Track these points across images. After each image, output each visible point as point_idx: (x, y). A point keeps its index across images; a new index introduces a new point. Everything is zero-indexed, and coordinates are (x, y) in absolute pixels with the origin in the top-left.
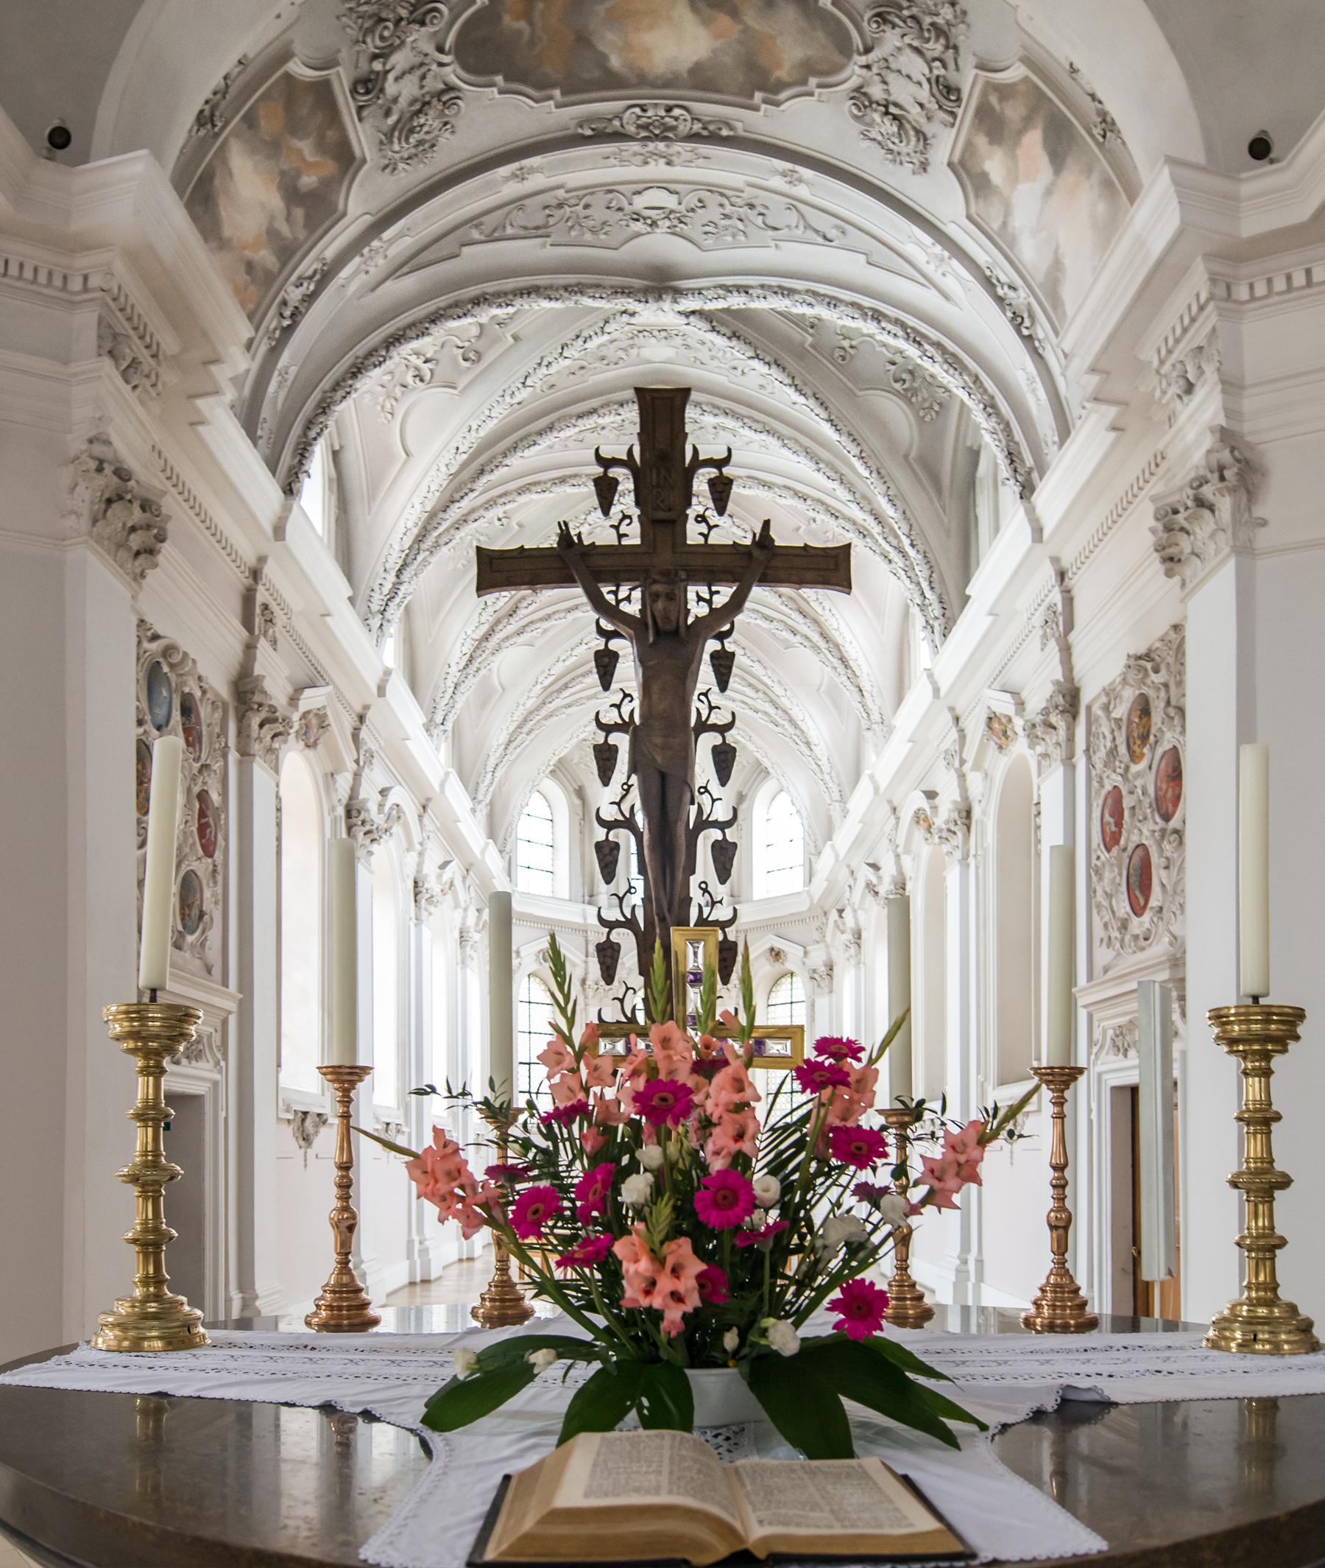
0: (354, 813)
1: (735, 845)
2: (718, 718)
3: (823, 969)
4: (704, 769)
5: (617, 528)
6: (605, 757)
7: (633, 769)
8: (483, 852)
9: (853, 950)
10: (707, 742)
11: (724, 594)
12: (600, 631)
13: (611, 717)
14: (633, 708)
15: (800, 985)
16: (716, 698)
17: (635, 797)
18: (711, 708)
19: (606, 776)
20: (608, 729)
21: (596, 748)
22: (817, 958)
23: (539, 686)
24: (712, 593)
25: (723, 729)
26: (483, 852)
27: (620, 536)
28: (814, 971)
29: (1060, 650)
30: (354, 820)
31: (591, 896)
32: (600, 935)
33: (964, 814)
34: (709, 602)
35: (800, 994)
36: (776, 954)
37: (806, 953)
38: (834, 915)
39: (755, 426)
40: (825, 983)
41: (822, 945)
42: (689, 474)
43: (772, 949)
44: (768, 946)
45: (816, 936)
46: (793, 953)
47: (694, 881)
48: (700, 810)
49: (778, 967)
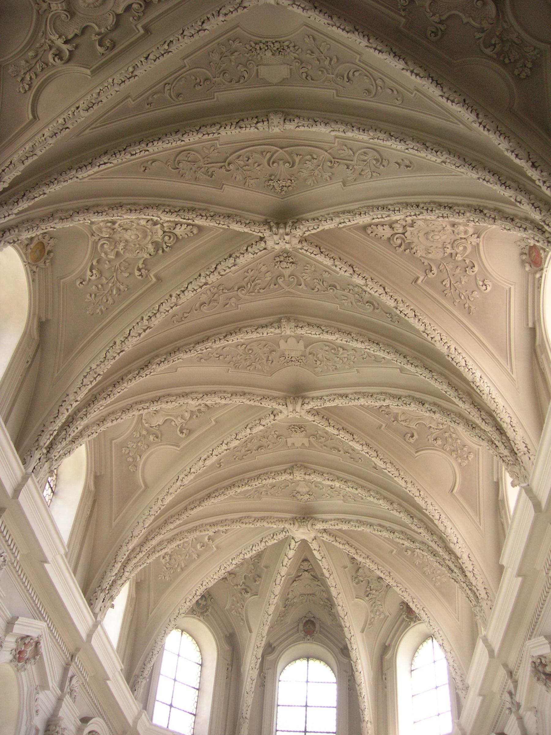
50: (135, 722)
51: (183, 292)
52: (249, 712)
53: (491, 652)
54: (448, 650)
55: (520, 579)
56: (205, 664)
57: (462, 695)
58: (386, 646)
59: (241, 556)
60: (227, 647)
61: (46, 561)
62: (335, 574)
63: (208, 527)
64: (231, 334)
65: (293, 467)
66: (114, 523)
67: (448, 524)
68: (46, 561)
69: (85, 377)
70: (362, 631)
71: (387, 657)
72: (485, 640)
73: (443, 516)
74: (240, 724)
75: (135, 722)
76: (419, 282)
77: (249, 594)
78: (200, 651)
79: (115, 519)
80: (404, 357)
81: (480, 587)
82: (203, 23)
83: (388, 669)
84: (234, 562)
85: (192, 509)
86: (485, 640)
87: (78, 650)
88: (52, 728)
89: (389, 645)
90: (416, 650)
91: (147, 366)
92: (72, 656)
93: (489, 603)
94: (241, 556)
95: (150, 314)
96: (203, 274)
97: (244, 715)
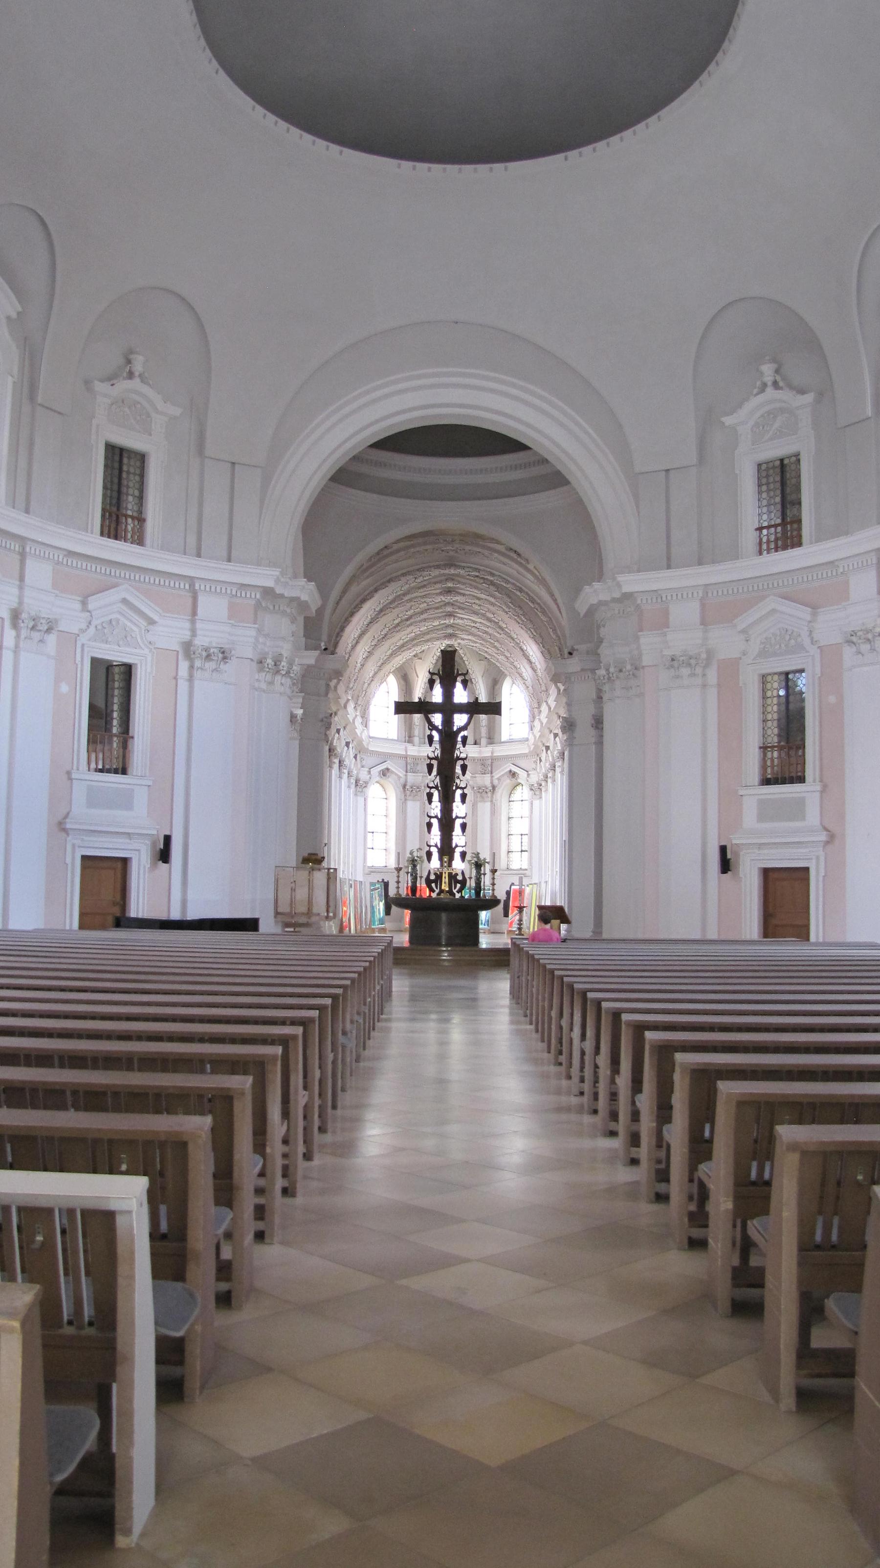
0: (332, 751)
1: (466, 794)
2: (463, 756)
3: (536, 785)
4: (458, 770)
6: (430, 768)
7: (438, 774)
10: (460, 763)
12: (429, 729)
13: (432, 755)
14: (438, 752)
16: (462, 749)
17: (438, 780)
18: (461, 753)
19: (430, 772)
20: (431, 759)
21: (427, 764)
23: (391, 651)
25: (463, 759)
28: (533, 785)
30: (331, 753)
31: (410, 737)
32: (427, 820)
33: (562, 754)
36: (513, 774)
37: (528, 775)
39: (486, 593)
40: (537, 793)
43: (510, 771)
44: (508, 769)
45: (534, 766)
46: (522, 774)
47: (454, 804)
48: (457, 784)
60: (403, 682)
61: (356, 728)
62: (468, 654)
65: (446, 626)
68: (356, 728)
70: (482, 677)
71: (497, 687)
72: (539, 719)
83: (497, 695)
86: (539, 719)
88: (351, 773)
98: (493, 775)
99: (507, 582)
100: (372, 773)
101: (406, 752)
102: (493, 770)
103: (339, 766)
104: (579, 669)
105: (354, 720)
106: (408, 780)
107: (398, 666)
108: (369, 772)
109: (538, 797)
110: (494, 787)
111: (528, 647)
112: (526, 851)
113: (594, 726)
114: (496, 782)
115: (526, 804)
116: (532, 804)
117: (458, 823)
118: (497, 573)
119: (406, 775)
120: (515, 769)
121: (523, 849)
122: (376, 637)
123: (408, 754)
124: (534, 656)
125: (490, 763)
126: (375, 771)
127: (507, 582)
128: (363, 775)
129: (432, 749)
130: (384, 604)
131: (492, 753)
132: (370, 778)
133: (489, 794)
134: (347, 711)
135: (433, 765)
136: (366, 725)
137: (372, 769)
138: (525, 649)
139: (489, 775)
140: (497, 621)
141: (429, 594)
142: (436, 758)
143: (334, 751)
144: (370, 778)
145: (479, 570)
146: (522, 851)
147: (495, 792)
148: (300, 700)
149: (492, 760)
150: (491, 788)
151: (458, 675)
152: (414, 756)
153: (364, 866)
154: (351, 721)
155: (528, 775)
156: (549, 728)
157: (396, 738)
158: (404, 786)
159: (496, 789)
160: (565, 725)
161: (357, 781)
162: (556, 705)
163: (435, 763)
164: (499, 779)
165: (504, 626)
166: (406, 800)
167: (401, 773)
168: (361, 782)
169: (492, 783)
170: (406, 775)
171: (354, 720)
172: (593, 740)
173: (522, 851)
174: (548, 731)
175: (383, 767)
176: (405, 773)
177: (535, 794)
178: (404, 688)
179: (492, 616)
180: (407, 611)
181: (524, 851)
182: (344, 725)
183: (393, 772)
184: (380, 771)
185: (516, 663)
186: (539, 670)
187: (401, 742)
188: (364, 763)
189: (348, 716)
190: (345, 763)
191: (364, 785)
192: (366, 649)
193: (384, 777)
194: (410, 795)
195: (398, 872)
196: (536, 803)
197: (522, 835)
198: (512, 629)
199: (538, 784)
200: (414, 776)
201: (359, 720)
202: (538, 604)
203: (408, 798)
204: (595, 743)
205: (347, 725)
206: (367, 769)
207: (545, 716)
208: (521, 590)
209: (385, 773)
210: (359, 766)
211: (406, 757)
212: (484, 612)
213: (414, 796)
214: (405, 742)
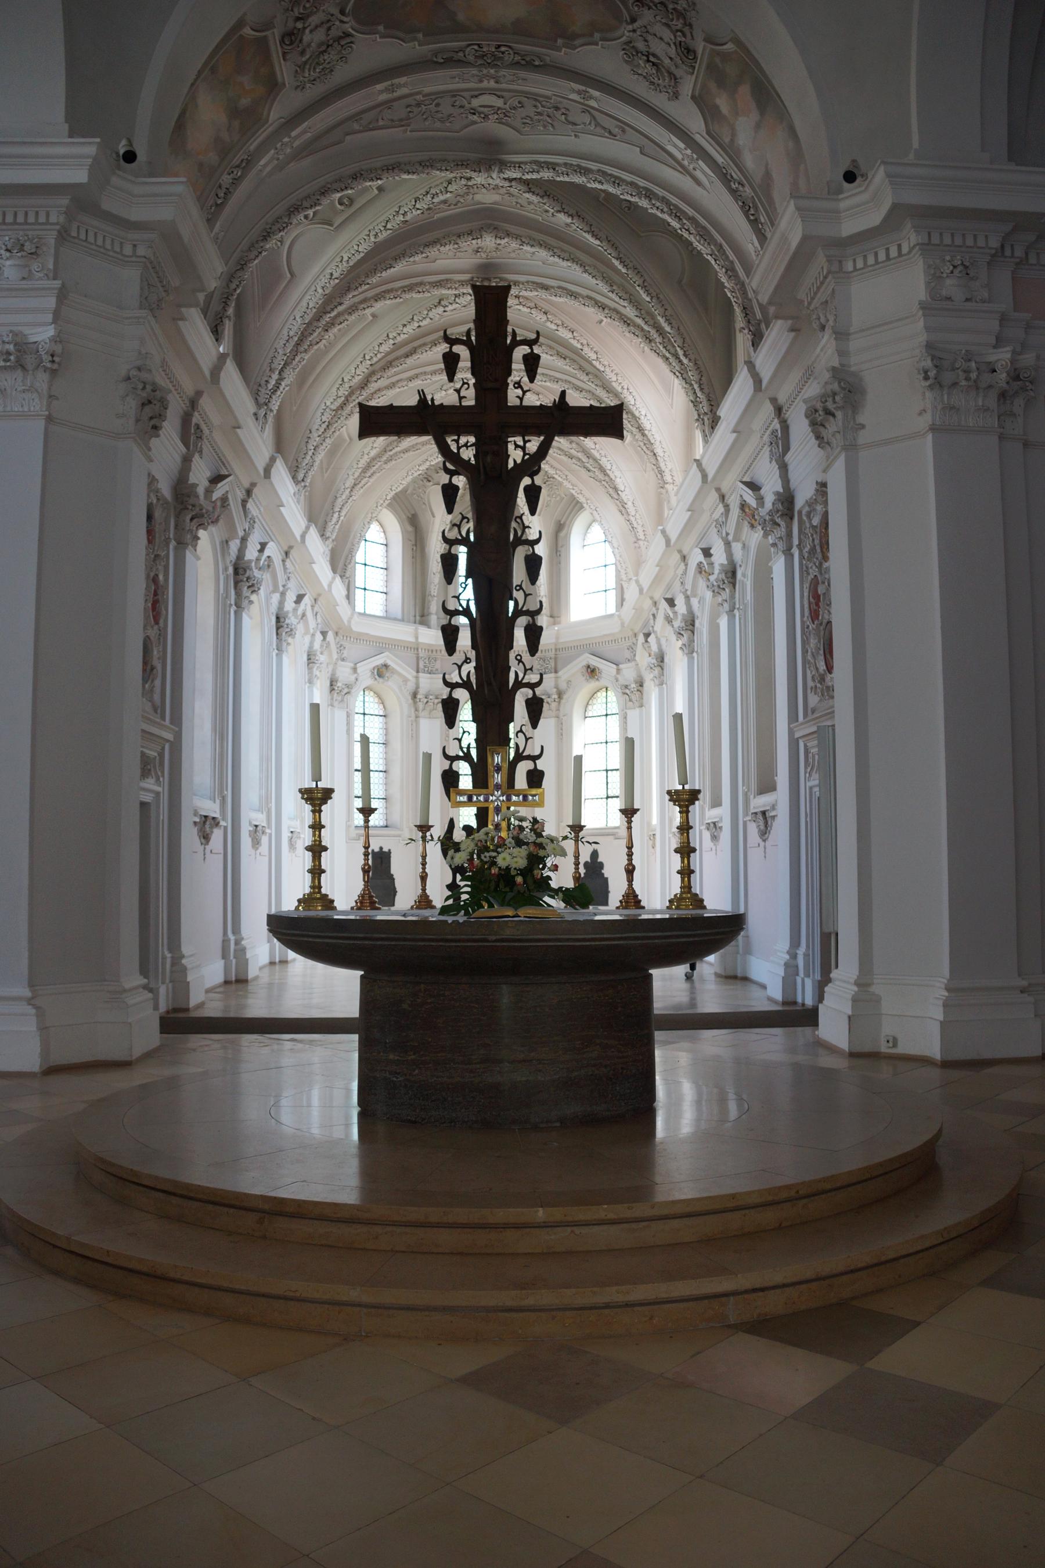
3: (633, 685)
5: (458, 391)
8: (330, 585)
9: (657, 670)
11: (533, 446)
15: (614, 699)
22: (628, 673)
24: (525, 442)
26: (330, 585)
27: (461, 398)
28: (626, 687)
29: (779, 468)
31: (422, 616)
33: (730, 575)
34: (523, 448)
35: (614, 707)
37: (618, 671)
38: (641, 638)
41: (633, 663)
42: (509, 351)
43: (589, 667)
44: (584, 663)
45: (627, 654)
46: (607, 669)
49: (593, 685)
50: (349, 622)
51: (399, 334)
52: (436, 591)
53: (641, 591)
54: (616, 545)
55: (658, 568)
56: (390, 545)
57: (625, 586)
58: (561, 524)
59: (428, 463)
60: (410, 529)
63: (402, 455)
64: (436, 345)
66: (326, 475)
67: (618, 474)
69: (323, 414)
71: (562, 534)
73: (614, 467)
74: (429, 602)
75: (349, 622)
76: (603, 323)
77: (431, 483)
78: (384, 532)
79: (327, 470)
80: (587, 374)
81: (640, 529)
82: (433, 198)
84: (421, 468)
85: (391, 450)
87: (319, 595)
88: (312, 657)
89: (564, 523)
90: (589, 526)
91: (366, 385)
92: (315, 600)
93: (646, 543)
94: (428, 463)
95: (371, 355)
96: (415, 318)
97: (432, 593)
98: (560, 673)
99: (617, 181)
100: (359, 671)
101: (417, 638)
102: (559, 666)
103: (278, 628)
104: (875, 218)
105: (303, 536)
106: (421, 685)
107: (399, 489)
108: (355, 670)
109: (637, 704)
110: (560, 694)
111: (637, 397)
112: (617, 797)
113: (932, 374)
114: (563, 686)
115: (614, 722)
116: (625, 718)
117: (520, 698)
118: (594, 166)
119: (417, 678)
120: (595, 662)
121: (610, 794)
122: (346, 380)
123: (420, 640)
124: (649, 416)
125: (553, 656)
126: (365, 669)
127: (617, 181)
128: (344, 673)
129: (455, 517)
130: (351, 263)
131: (557, 638)
132: (357, 679)
133: (554, 705)
134: (272, 484)
135: (455, 558)
136: (349, 597)
137: (358, 665)
138: (632, 403)
139: (553, 675)
140: (579, 346)
141: (447, 280)
142: (466, 685)
143: (245, 571)
144: (357, 679)
145: (552, 166)
146: (608, 797)
147: (563, 701)
148: (51, 302)
149: (556, 650)
150: (556, 696)
151: (516, 343)
152: (430, 645)
153: (348, 827)
154: (299, 538)
155: (618, 671)
156: (651, 598)
157: (399, 616)
158: (415, 695)
159: (565, 697)
160: (835, 386)
161: (332, 683)
162: (736, 441)
163: (462, 553)
164: (569, 682)
165: (593, 356)
166: (417, 717)
167: (409, 673)
168: (339, 684)
169: (556, 687)
170: (417, 678)
171: (303, 536)
172: (927, 419)
173: (608, 797)
174: (677, 557)
175: (378, 661)
176: (415, 673)
177: (630, 700)
178: (413, 538)
179: (570, 335)
180: (404, 325)
181: (612, 797)
182: (247, 485)
183: (394, 671)
184: (374, 669)
185: (604, 462)
186: (658, 443)
187: (409, 622)
188: (345, 653)
189: (282, 508)
190: (287, 621)
191: (346, 690)
192: (328, 403)
193: (381, 680)
194: (424, 709)
195: (317, 811)
196: (633, 714)
197: (607, 771)
198: (606, 363)
199: (636, 683)
200: (431, 678)
201: (317, 548)
202: (692, 219)
203: (421, 714)
204: (933, 429)
205: (291, 547)
206: (352, 665)
207: (687, 507)
208: (649, 195)
209: (381, 671)
210: (335, 656)
211: (416, 648)
212: (554, 327)
213: (431, 711)
214: (415, 623)
